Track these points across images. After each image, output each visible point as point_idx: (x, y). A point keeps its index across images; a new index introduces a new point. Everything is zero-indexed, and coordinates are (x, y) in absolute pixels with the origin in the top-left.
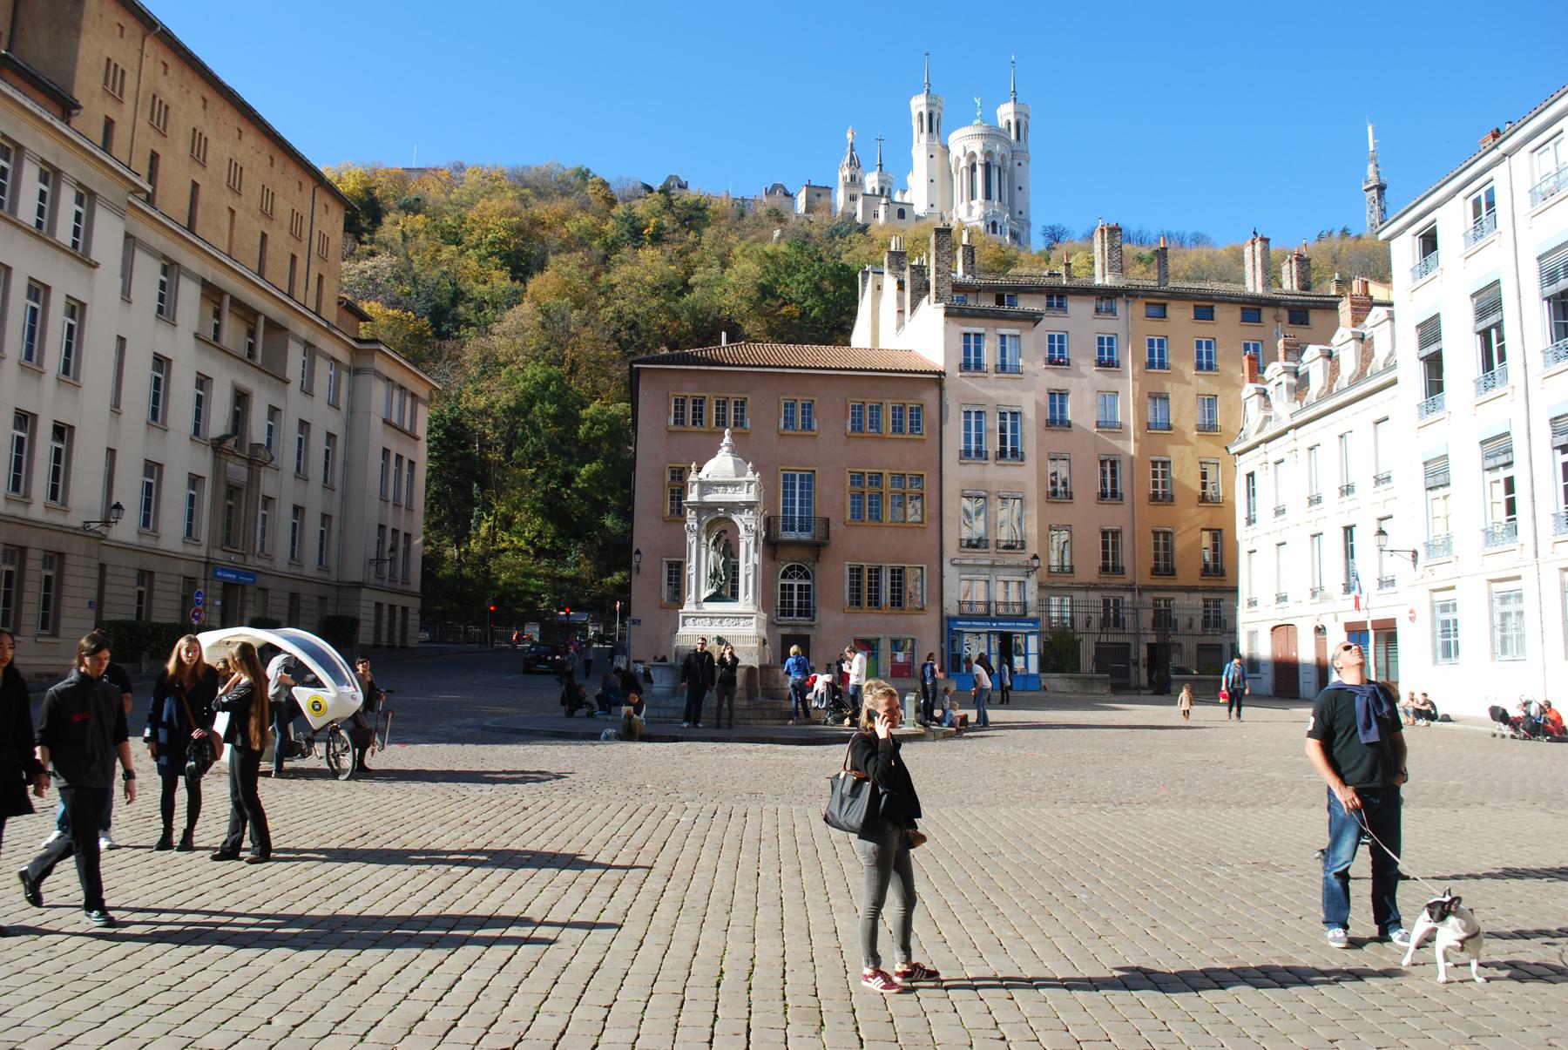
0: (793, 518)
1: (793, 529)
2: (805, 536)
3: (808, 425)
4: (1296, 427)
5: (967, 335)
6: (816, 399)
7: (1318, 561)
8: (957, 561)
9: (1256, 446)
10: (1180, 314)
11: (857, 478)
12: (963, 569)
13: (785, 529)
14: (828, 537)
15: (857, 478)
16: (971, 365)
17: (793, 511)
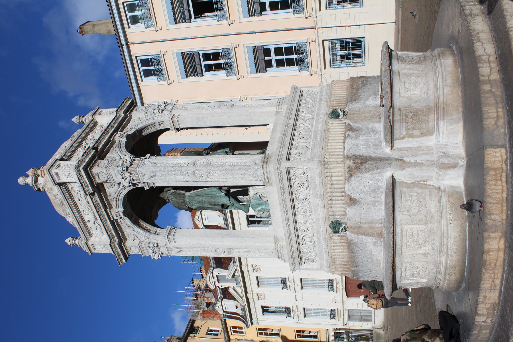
4: (241, 264)
9: (248, 300)
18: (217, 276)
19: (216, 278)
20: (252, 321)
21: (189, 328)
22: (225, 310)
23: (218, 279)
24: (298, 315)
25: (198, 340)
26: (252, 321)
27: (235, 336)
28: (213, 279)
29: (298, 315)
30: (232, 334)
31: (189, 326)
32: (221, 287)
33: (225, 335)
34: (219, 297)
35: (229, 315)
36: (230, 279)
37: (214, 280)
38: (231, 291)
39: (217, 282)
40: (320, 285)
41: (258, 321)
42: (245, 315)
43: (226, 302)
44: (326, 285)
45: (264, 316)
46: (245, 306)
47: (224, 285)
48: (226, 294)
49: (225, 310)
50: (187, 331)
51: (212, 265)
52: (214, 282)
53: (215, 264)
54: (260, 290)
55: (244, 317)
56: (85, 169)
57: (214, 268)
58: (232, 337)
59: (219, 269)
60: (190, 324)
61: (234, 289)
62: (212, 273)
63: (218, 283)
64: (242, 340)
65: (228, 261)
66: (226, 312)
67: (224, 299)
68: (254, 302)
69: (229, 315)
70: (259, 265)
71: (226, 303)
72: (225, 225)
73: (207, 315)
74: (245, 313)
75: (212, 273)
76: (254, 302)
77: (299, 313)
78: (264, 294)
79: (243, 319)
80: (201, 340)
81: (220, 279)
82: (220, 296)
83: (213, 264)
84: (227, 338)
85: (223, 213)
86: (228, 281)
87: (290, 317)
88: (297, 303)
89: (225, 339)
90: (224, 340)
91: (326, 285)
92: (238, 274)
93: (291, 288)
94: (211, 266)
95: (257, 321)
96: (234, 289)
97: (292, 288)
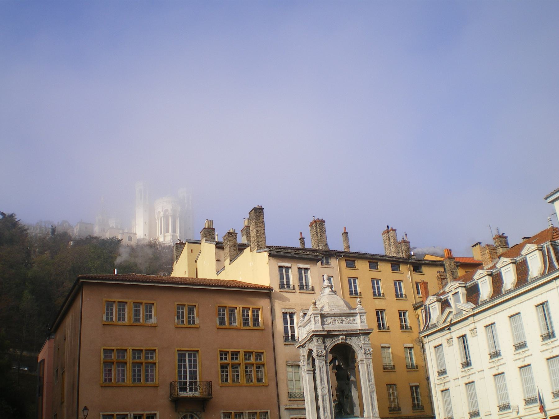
0: (185, 383)
1: (185, 390)
2: (196, 394)
3: (191, 320)
4: (473, 315)
5: (281, 267)
6: (197, 304)
7: (501, 390)
8: (288, 407)
10: (362, 266)
11: (223, 355)
12: (292, 412)
13: (181, 389)
14: (210, 394)
15: (223, 355)
16: (284, 285)
17: (185, 377)
18: (458, 292)
19: (456, 291)
20: (426, 337)
21: (418, 262)
22: (430, 306)
23: (455, 293)
24: (441, 384)
25: (408, 276)
26: (426, 337)
27: (421, 314)
28: (455, 289)
29: (441, 384)
30: (422, 310)
31: (421, 262)
32: (449, 298)
33: (419, 303)
34: (441, 297)
35: (428, 311)
36: (458, 307)
37: (453, 290)
38: (447, 310)
39: (453, 293)
40: (473, 403)
41: (428, 343)
42: (430, 329)
43: (437, 305)
44: (474, 408)
45: (434, 348)
46: (437, 327)
47: (452, 302)
48: (445, 304)
49: (430, 306)
50: (414, 262)
51: (468, 285)
52: (452, 291)
53: (469, 287)
54: (455, 340)
55: (428, 328)
56: (313, 335)
57: (465, 287)
58: (419, 311)
59: (465, 292)
60: (423, 262)
61: (450, 313)
62: (460, 287)
63: (453, 295)
64: (419, 322)
65: (475, 300)
66: (429, 306)
67: (440, 303)
68: (444, 336)
69: (428, 311)
70: (477, 335)
71: (437, 306)
72: (505, 291)
73: (423, 288)
74: (432, 328)
75: (460, 287)
76: (444, 336)
77: (443, 385)
78: (453, 345)
79: (426, 327)
80: (409, 278)
81: (455, 296)
82: (442, 298)
83: (469, 285)
84: (417, 306)
85: (515, 287)
86: (456, 305)
87: (438, 376)
88: (452, 381)
89: (416, 304)
90: (415, 303)
91: (474, 408)
92: (465, 314)
93: (464, 373)
94: (466, 284)
95: (427, 342)
96: (450, 313)
97: (464, 374)
